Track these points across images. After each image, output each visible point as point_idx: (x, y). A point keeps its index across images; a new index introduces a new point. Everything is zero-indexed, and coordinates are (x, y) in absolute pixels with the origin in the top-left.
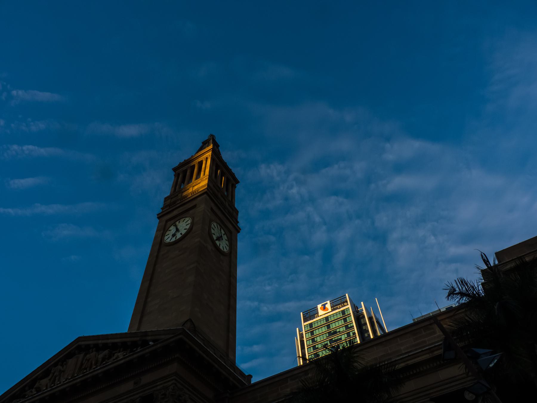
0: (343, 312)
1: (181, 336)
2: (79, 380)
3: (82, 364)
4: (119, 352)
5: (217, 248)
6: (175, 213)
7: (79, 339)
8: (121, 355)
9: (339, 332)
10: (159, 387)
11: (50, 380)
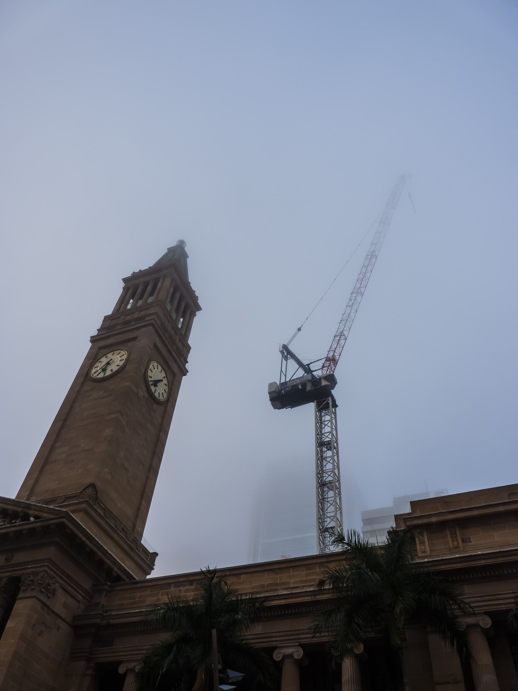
5: (151, 395)
6: (112, 340)
10: (29, 571)
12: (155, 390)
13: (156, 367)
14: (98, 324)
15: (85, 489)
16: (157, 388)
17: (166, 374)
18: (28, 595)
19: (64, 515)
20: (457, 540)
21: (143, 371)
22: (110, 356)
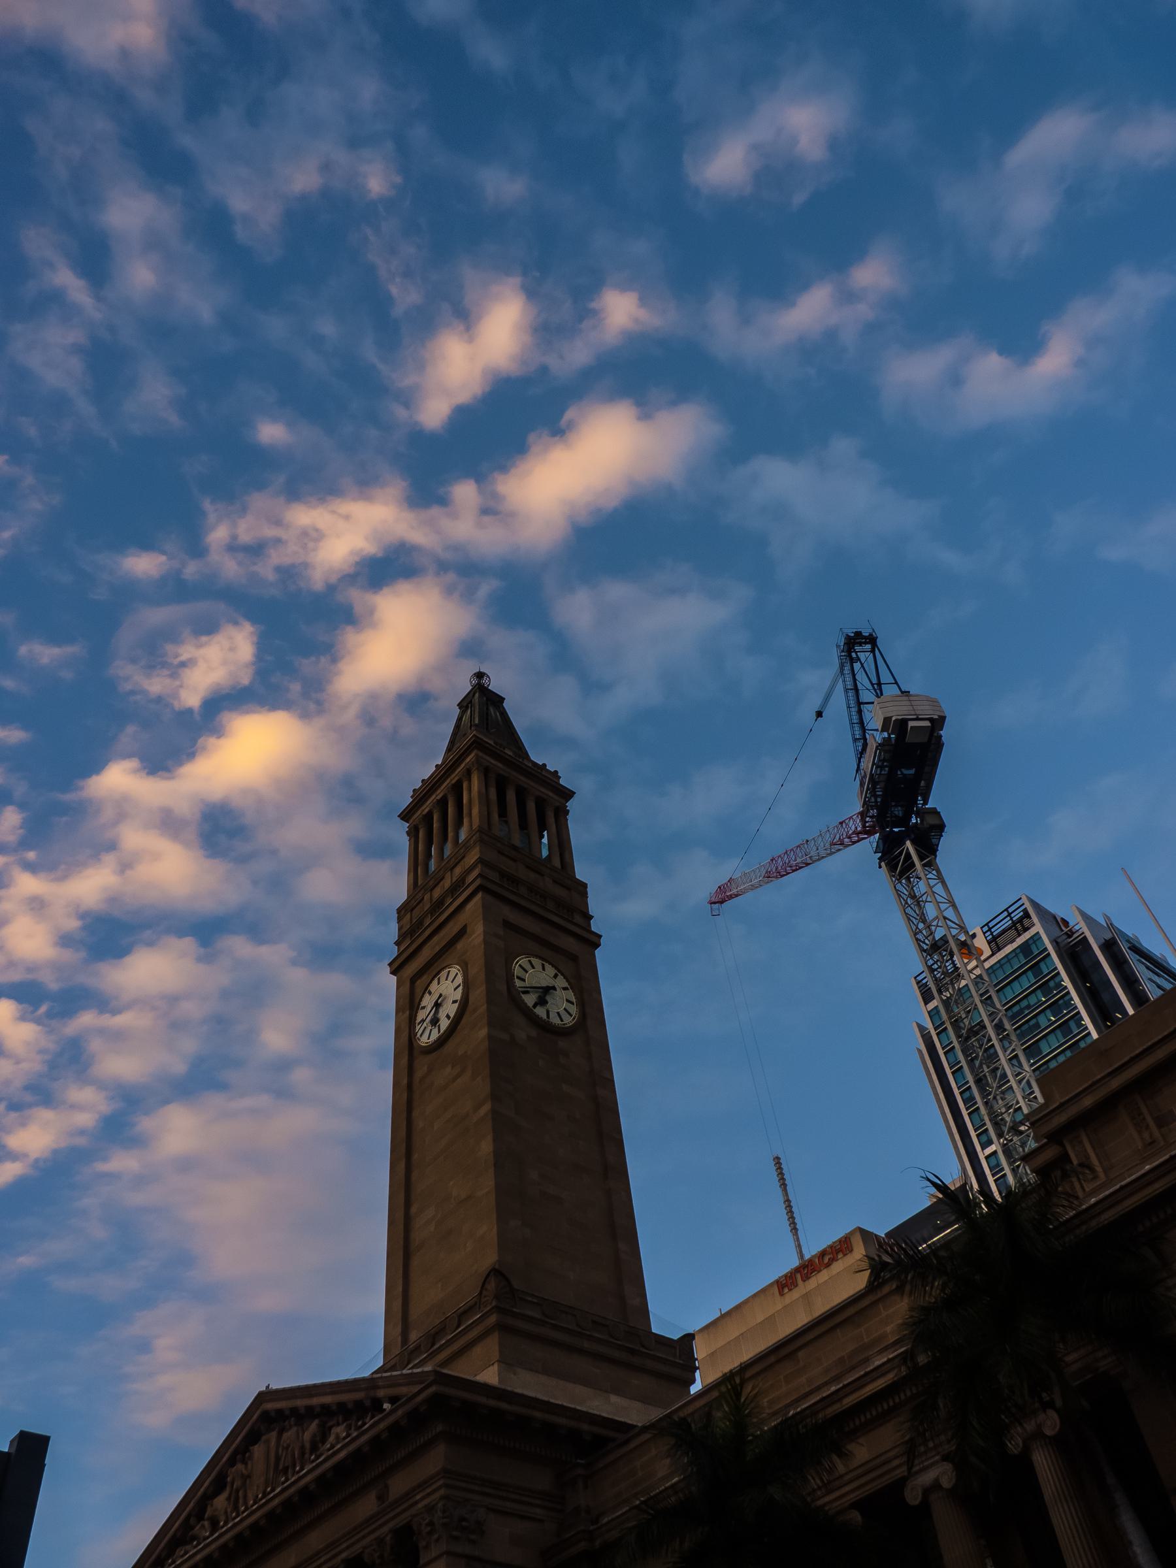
0: (1025, 948)
1: (433, 1389)
2: (276, 1502)
3: (278, 1458)
4: (338, 1424)
5: (544, 1027)
7: (264, 1397)
8: (340, 1430)
9: (1028, 1007)
10: (420, 1506)
11: (228, 1499)
12: (548, 1012)
13: (527, 966)
14: (392, 930)
17: (556, 968)
18: (434, 1555)
19: (431, 1378)
20: (1147, 1127)
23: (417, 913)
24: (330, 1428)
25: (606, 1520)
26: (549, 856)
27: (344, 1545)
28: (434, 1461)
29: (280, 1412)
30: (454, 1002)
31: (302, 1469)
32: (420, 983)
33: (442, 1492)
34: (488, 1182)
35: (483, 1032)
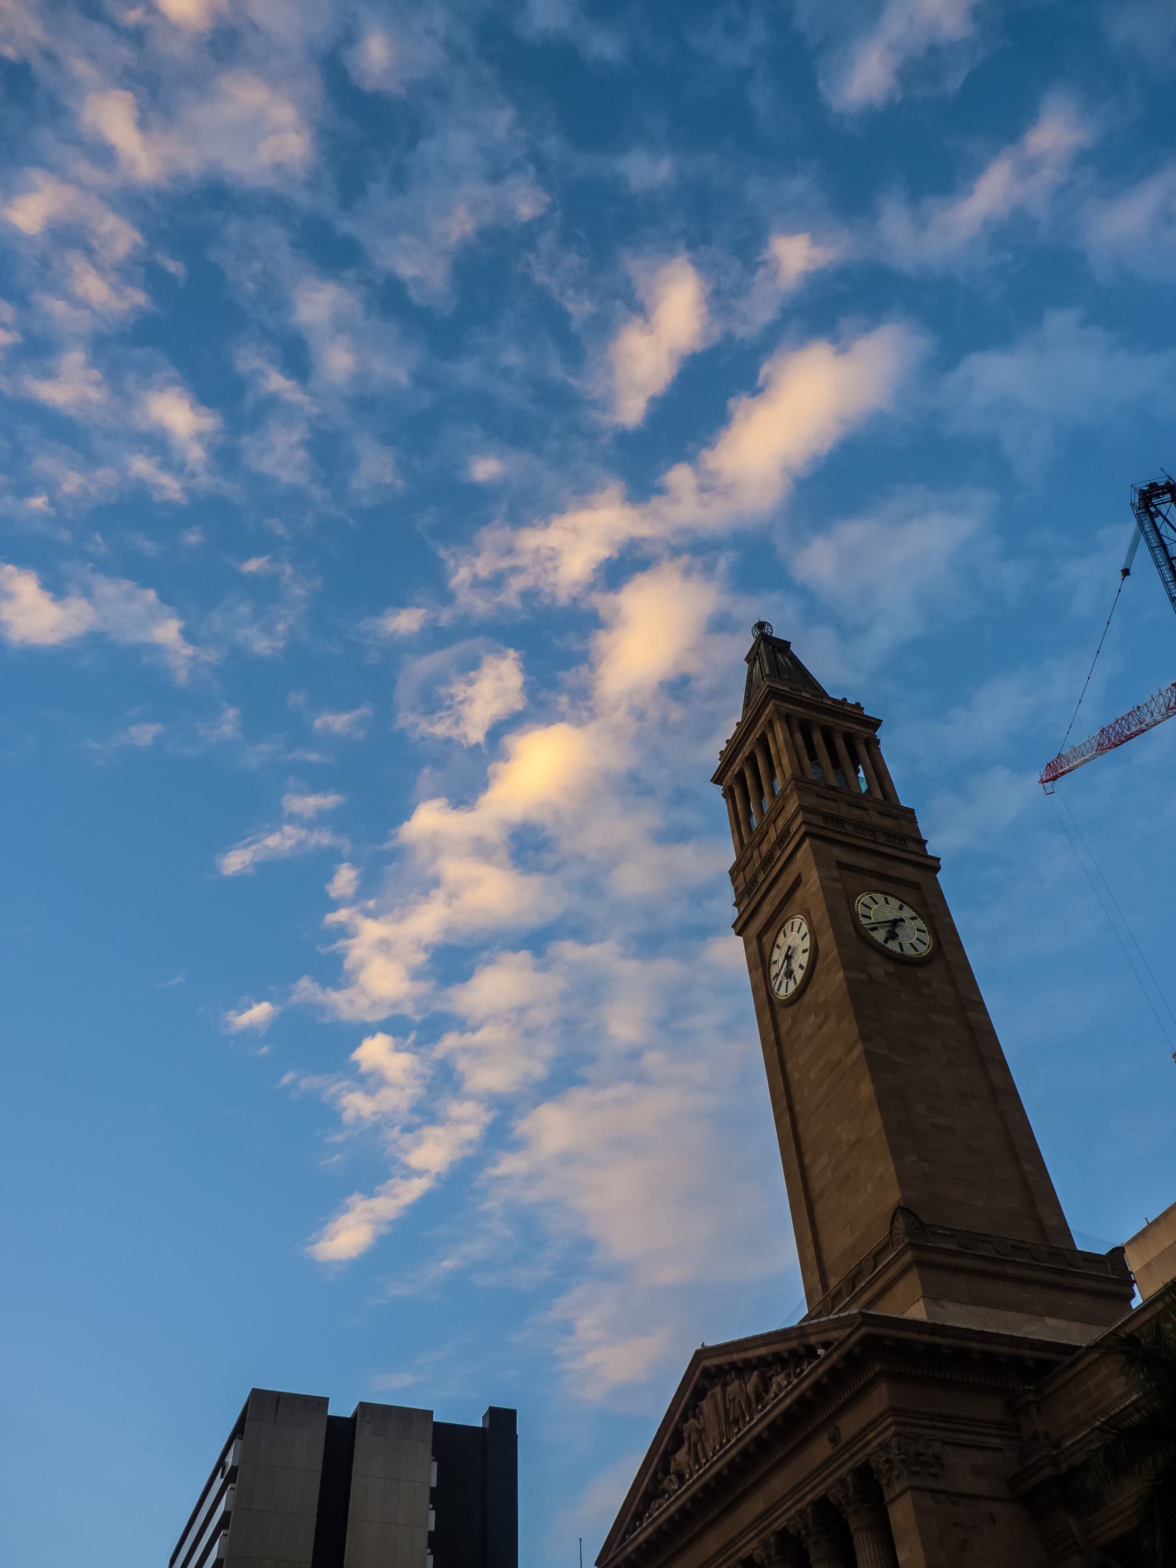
1: (863, 1330)
2: (734, 1452)
3: (727, 1412)
4: (778, 1374)
6: (767, 909)
7: (701, 1355)
8: (780, 1379)
10: (874, 1444)
11: (689, 1453)
12: (901, 945)
15: (892, 1222)
16: (901, 939)
18: (897, 1491)
19: (860, 1320)
21: (851, 929)
22: (781, 940)
23: (749, 872)
24: (771, 1378)
25: (1068, 1443)
26: (869, 790)
27: (808, 1488)
28: (879, 1399)
29: (719, 1367)
30: (804, 951)
31: (752, 1419)
32: (767, 939)
33: (893, 1429)
34: (876, 1121)
35: (840, 975)
